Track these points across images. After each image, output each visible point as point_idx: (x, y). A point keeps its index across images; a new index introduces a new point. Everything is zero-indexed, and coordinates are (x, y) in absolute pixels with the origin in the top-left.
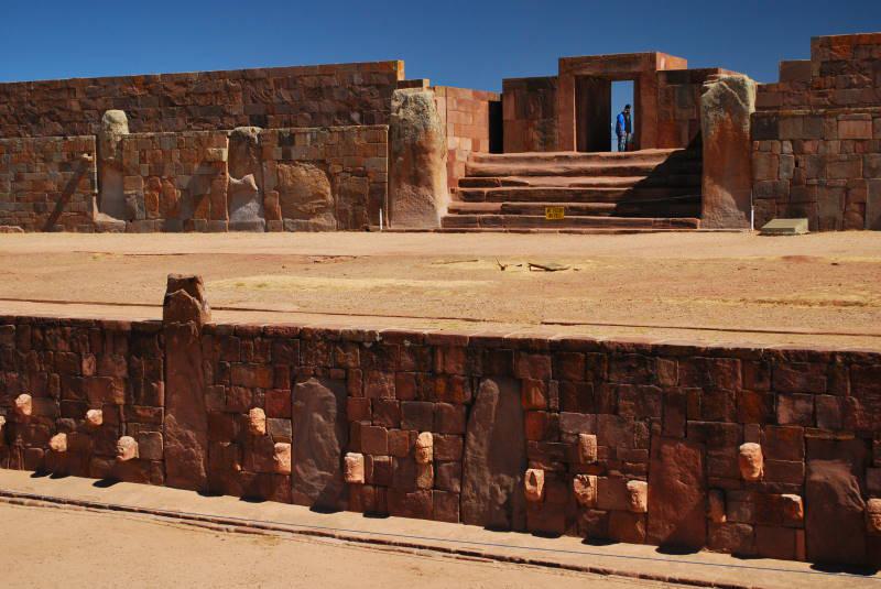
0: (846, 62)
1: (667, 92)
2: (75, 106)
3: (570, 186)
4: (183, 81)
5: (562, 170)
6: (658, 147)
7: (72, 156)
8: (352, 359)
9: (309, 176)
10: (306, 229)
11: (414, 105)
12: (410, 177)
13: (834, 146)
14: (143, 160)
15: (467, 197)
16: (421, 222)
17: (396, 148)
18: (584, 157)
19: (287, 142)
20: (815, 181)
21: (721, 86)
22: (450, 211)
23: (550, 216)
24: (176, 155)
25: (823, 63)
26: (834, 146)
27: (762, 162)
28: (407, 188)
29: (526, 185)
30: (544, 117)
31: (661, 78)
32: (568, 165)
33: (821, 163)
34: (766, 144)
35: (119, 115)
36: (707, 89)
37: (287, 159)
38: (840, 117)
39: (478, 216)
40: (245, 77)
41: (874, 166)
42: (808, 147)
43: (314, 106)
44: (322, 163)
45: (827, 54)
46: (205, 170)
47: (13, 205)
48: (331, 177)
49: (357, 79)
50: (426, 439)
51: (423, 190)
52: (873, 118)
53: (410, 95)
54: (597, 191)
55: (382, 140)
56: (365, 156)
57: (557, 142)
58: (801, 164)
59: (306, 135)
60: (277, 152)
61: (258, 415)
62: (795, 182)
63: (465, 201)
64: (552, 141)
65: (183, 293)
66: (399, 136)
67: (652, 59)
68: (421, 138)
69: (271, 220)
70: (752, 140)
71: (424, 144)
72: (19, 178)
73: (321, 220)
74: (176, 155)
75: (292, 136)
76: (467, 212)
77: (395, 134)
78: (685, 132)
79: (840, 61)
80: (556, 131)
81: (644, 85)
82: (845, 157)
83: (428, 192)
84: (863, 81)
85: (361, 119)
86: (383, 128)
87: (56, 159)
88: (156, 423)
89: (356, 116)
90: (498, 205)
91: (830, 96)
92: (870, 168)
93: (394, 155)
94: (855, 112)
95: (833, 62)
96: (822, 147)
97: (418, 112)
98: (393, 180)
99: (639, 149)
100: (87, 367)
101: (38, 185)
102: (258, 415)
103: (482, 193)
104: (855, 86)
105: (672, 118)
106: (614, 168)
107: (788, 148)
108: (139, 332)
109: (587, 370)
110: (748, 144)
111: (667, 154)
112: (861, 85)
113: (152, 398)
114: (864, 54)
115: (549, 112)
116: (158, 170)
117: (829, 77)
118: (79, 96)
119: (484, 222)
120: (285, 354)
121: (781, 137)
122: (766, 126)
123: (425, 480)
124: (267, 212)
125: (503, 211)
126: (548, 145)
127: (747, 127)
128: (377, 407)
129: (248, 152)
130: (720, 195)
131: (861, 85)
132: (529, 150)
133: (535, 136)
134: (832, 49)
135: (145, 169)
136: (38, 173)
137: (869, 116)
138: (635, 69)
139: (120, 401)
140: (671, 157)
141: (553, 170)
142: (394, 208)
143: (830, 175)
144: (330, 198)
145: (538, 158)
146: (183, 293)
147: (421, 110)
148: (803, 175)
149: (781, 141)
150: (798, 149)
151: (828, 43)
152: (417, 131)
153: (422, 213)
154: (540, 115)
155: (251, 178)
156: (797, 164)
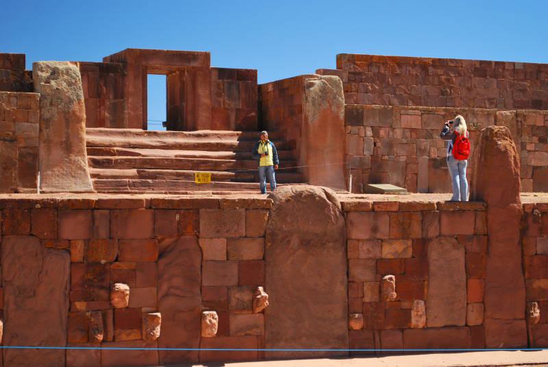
0: (365, 74)
1: (218, 85)
3: (176, 156)
5: (158, 144)
6: (212, 129)
11: (66, 77)
12: (61, 143)
13: (398, 132)
16: (74, 185)
17: (47, 115)
18: (170, 134)
20: (386, 157)
21: (324, 83)
22: (93, 176)
23: (199, 180)
25: (349, 73)
26: (398, 132)
27: (352, 142)
28: (57, 153)
29: (139, 155)
30: (115, 97)
31: (214, 76)
32: (159, 140)
33: (390, 145)
34: (355, 129)
36: (312, 85)
38: (402, 112)
39: (127, 180)
41: (423, 148)
42: (382, 132)
45: (352, 67)
51: (73, 157)
52: (422, 114)
53: (61, 67)
54: (212, 162)
55: (33, 106)
56: (14, 121)
57: (126, 122)
58: (379, 144)
62: (374, 157)
63: (94, 167)
64: (123, 119)
66: (51, 104)
67: (207, 56)
70: (345, 126)
71: (78, 113)
76: (107, 177)
77: (47, 102)
78: (233, 118)
79: (359, 74)
80: (126, 111)
81: (199, 79)
82: (404, 141)
83: (79, 158)
84: (375, 88)
86: (34, 96)
90: (134, 172)
91: (355, 98)
92: (420, 149)
93: (45, 122)
94: (411, 109)
95: (355, 74)
96: (391, 133)
97: (70, 84)
98: (42, 145)
99: (196, 130)
103: (111, 160)
104: (370, 92)
105: (222, 106)
106: (198, 144)
107: (369, 133)
110: (343, 128)
111: (238, 134)
112: (374, 91)
114: (375, 70)
115: (120, 94)
117: (354, 84)
121: (365, 124)
122: (355, 117)
127: (342, 116)
131: (374, 91)
132: (101, 126)
134: (355, 64)
137: (420, 113)
138: (194, 64)
141: (154, 144)
143: (397, 153)
145: (130, 133)
148: (380, 152)
149: (365, 127)
150: (376, 133)
151: (353, 59)
152: (71, 101)
153: (73, 177)
154: (111, 97)
156: (375, 145)
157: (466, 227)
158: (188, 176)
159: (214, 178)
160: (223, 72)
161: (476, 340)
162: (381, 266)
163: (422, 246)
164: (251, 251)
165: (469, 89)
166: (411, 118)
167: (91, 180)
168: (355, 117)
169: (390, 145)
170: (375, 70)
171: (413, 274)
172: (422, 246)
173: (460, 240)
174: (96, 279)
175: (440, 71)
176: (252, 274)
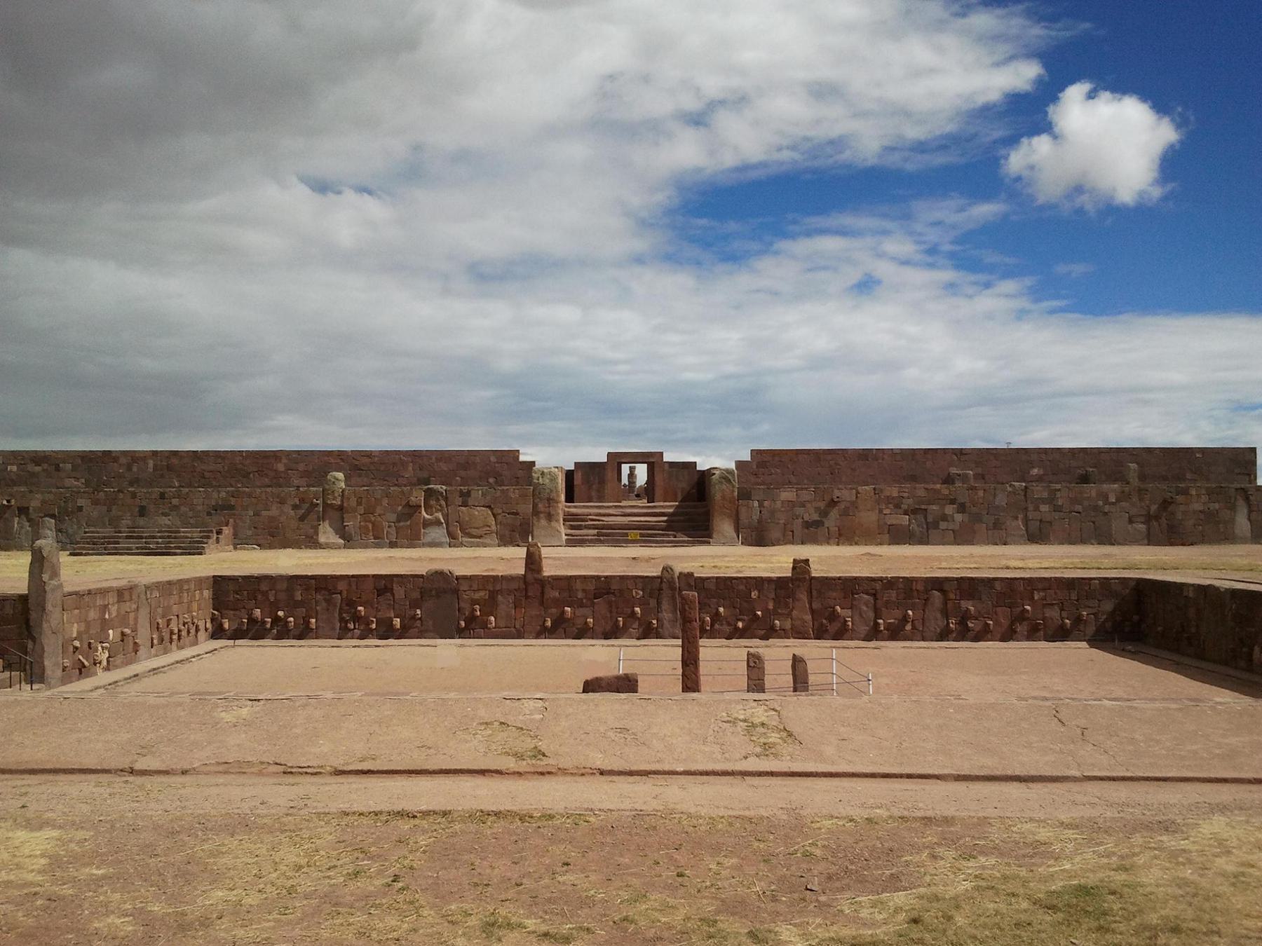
2: (281, 467)
4: (368, 454)
7: (302, 500)
8: (878, 586)
9: (480, 514)
10: (478, 546)
13: (779, 504)
14: (359, 504)
15: (572, 527)
19: (466, 495)
24: (385, 502)
26: (779, 504)
27: (743, 510)
28: (543, 522)
31: (666, 466)
33: (773, 512)
34: (745, 502)
35: (340, 475)
37: (465, 504)
40: (416, 455)
42: (766, 503)
43: (463, 473)
44: (489, 507)
46: (407, 510)
47: (250, 533)
48: (494, 515)
49: (493, 459)
50: (910, 612)
51: (554, 524)
59: (477, 493)
60: (459, 501)
61: (838, 608)
62: (760, 521)
65: (801, 566)
67: (661, 454)
68: (553, 495)
69: (453, 541)
72: (257, 514)
73: (488, 541)
74: (385, 502)
75: (468, 494)
81: (656, 470)
85: (496, 482)
87: (291, 502)
88: (789, 615)
89: (491, 480)
100: (754, 594)
101: (272, 519)
102: (838, 608)
107: (756, 504)
108: (780, 582)
109: (970, 587)
113: (787, 605)
115: (602, 482)
116: (369, 511)
118: (284, 461)
119: (591, 541)
120: (850, 587)
122: (745, 495)
123: (908, 627)
124: (451, 535)
125: (598, 535)
126: (601, 499)
128: (887, 604)
129: (438, 500)
130: (725, 527)
133: (594, 494)
135: (361, 510)
136: (274, 511)
139: (771, 606)
140: (677, 507)
142: (535, 533)
144: (494, 528)
146: (801, 566)
147: (553, 479)
150: (761, 505)
155: (440, 515)
157: (514, 585)
158: (627, 535)
159: (642, 535)
160: (672, 464)
161: (519, 635)
162: (474, 602)
163: (493, 595)
164: (416, 595)
165: (853, 470)
166: (787, 495)
167: (564, 538)
168: (745, 495)
169: (773, 512)
170: (777, 458)
171: (490, 605)
172: (493, 595)
173: (510, 592)
174: (351, 604)
175: (829, 457)
176: (415, 604)
